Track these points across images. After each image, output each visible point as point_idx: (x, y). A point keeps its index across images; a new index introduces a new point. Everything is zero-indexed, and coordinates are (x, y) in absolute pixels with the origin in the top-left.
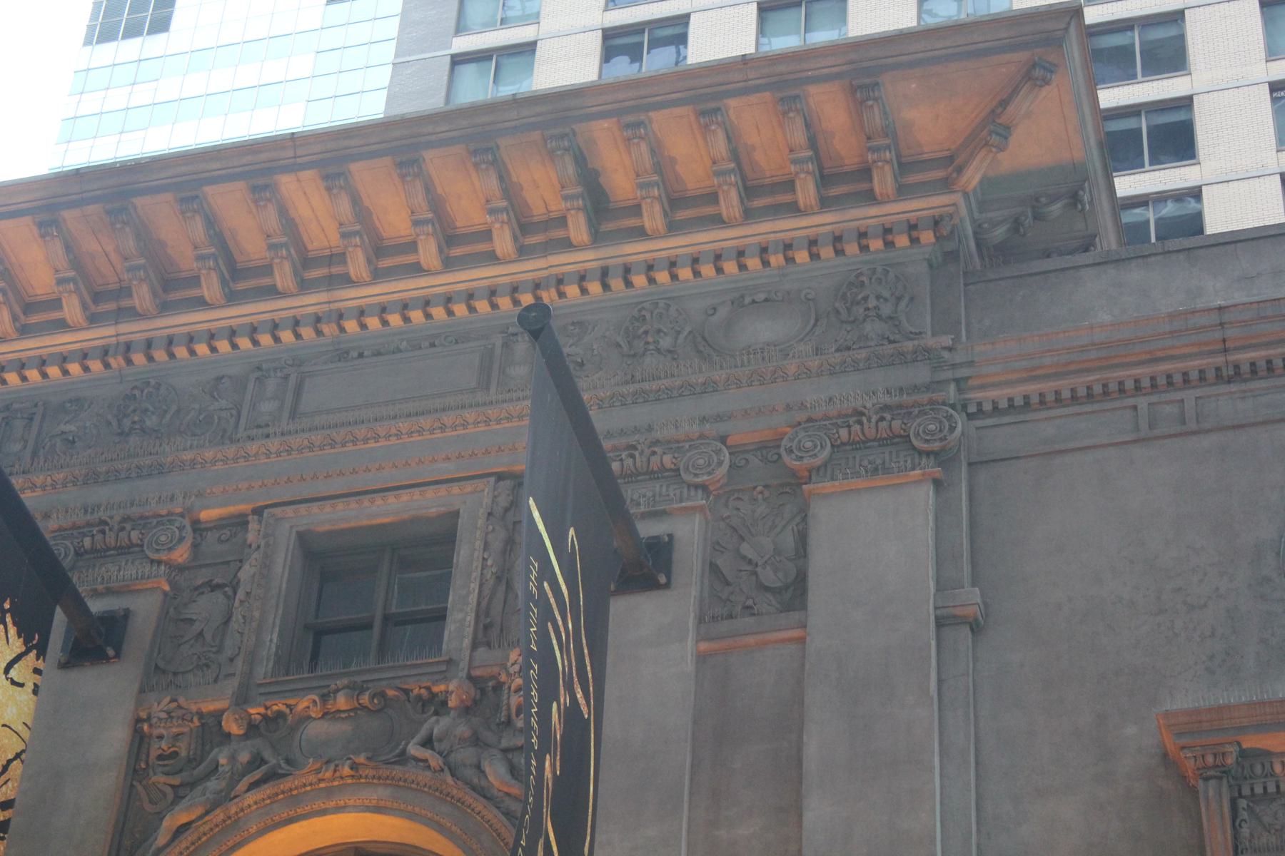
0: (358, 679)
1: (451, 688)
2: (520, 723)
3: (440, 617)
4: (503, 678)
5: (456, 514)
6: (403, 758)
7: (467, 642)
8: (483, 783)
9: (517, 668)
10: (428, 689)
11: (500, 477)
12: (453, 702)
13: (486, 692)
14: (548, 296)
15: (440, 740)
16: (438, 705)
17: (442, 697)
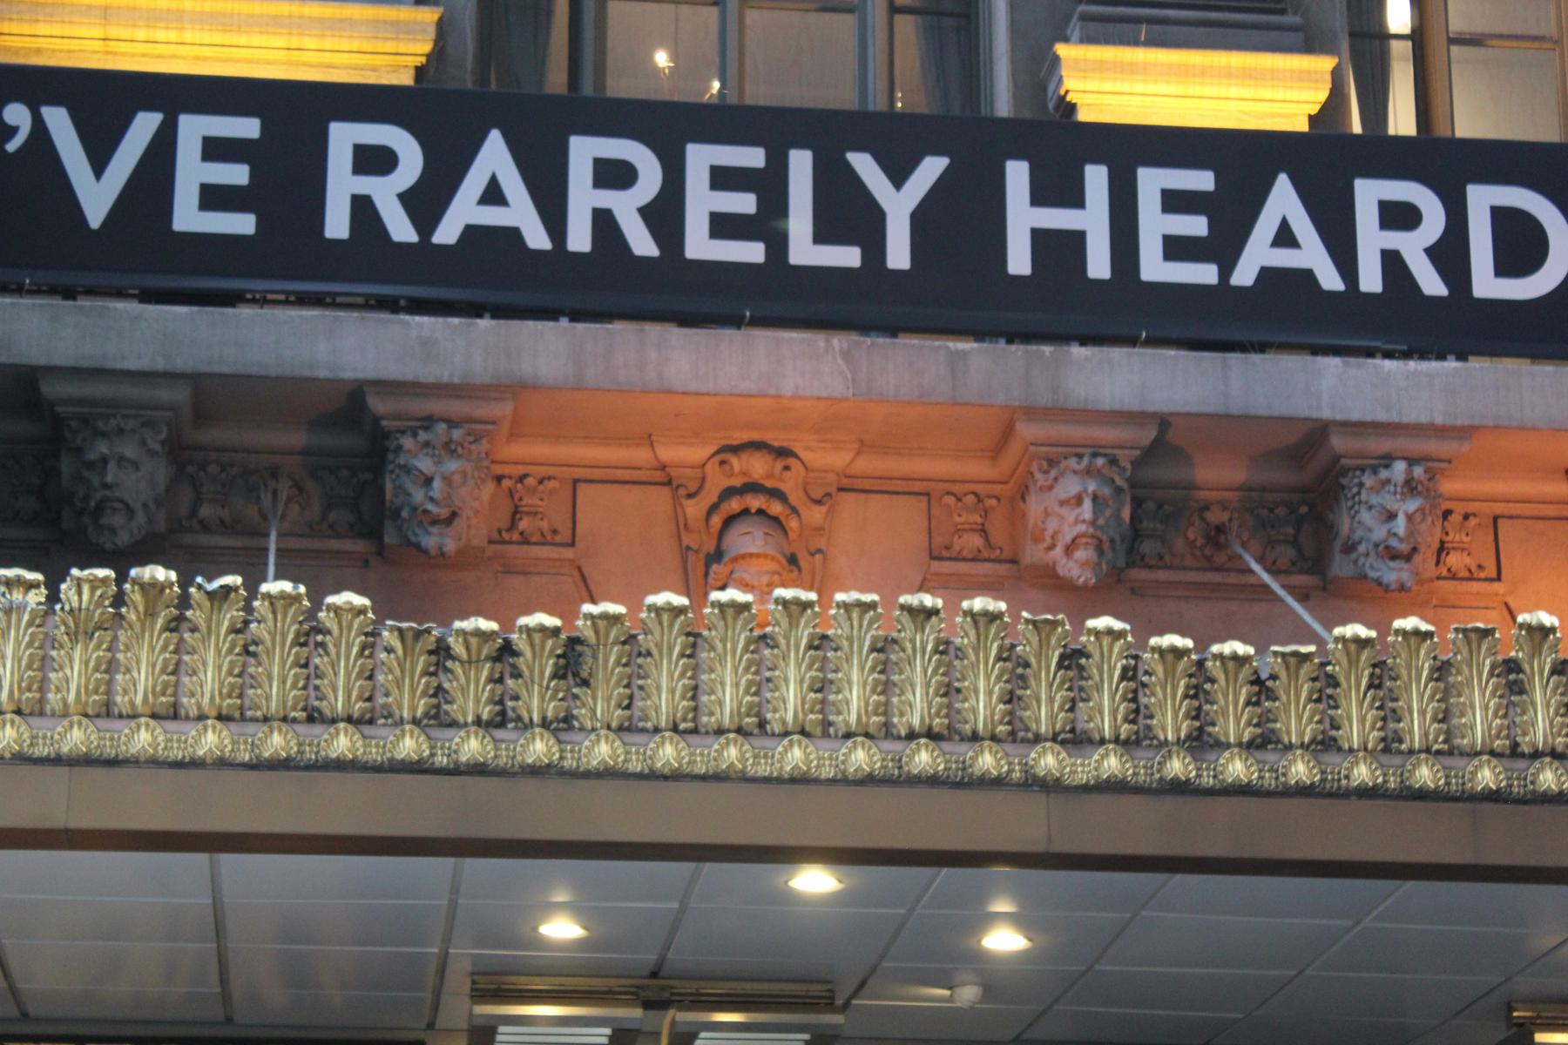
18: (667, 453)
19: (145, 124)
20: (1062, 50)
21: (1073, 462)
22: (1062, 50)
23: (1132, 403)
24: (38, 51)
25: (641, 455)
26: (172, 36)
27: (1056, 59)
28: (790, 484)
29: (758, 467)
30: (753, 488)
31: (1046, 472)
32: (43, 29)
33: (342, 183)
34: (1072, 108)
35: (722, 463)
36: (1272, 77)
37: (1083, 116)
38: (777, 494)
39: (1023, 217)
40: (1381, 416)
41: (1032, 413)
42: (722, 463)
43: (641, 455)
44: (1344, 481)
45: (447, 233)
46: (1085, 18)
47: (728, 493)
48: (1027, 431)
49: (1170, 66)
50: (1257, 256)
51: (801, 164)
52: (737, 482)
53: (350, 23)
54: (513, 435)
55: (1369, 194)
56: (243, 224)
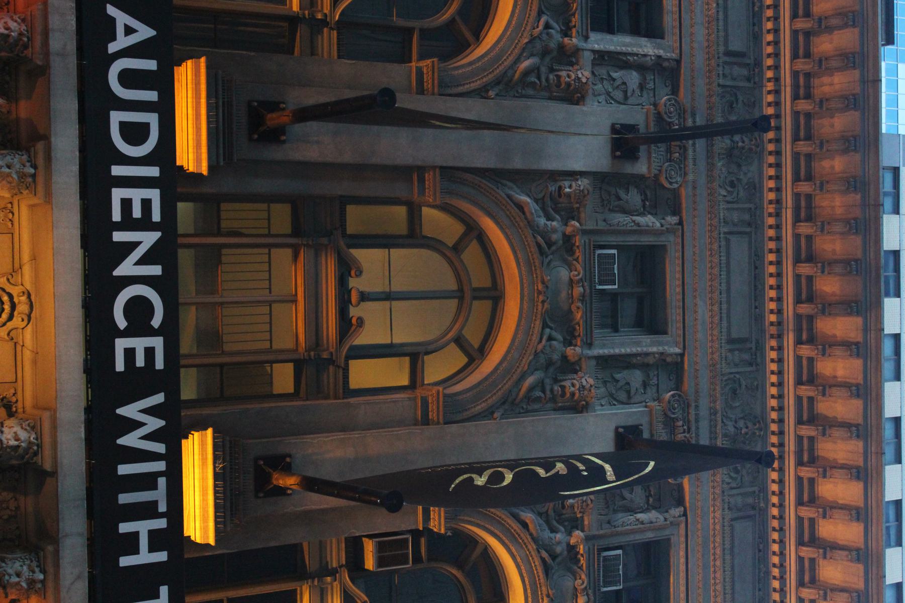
0: (587, 298)
1: (574, 40)
2: (556, 388)
3: (610, 31)
4: (576, 67)
5: (663, 38)
6: (540, 13)
7: (596, 47)
8: (523, 59)
9: (584, 383)
10: (579, 335)
11: (678, 62)
12: (566, 40)
13: (568, 57)
14: (771, 135)
15: (548, 34)
16: (566, 33)
17: (569, 33)
18: (27, 269)
20: (210, 431)
21: (33, 436)
22: (210, 431)
25: (26, 257)
27: (206, 429)
28: (17, 322)
29: (23, 308)
30: (13, 307)
31: (29, 425)
35: (24, 293)
36: (205, 519)
37: (184, 441)
38: (11, 317)
42: (24, 293)
43: (26, 257)
44: (33, 554)
47: (11, 296)
48: (46, 415)
52: (16, 300)
54: (32, 207)
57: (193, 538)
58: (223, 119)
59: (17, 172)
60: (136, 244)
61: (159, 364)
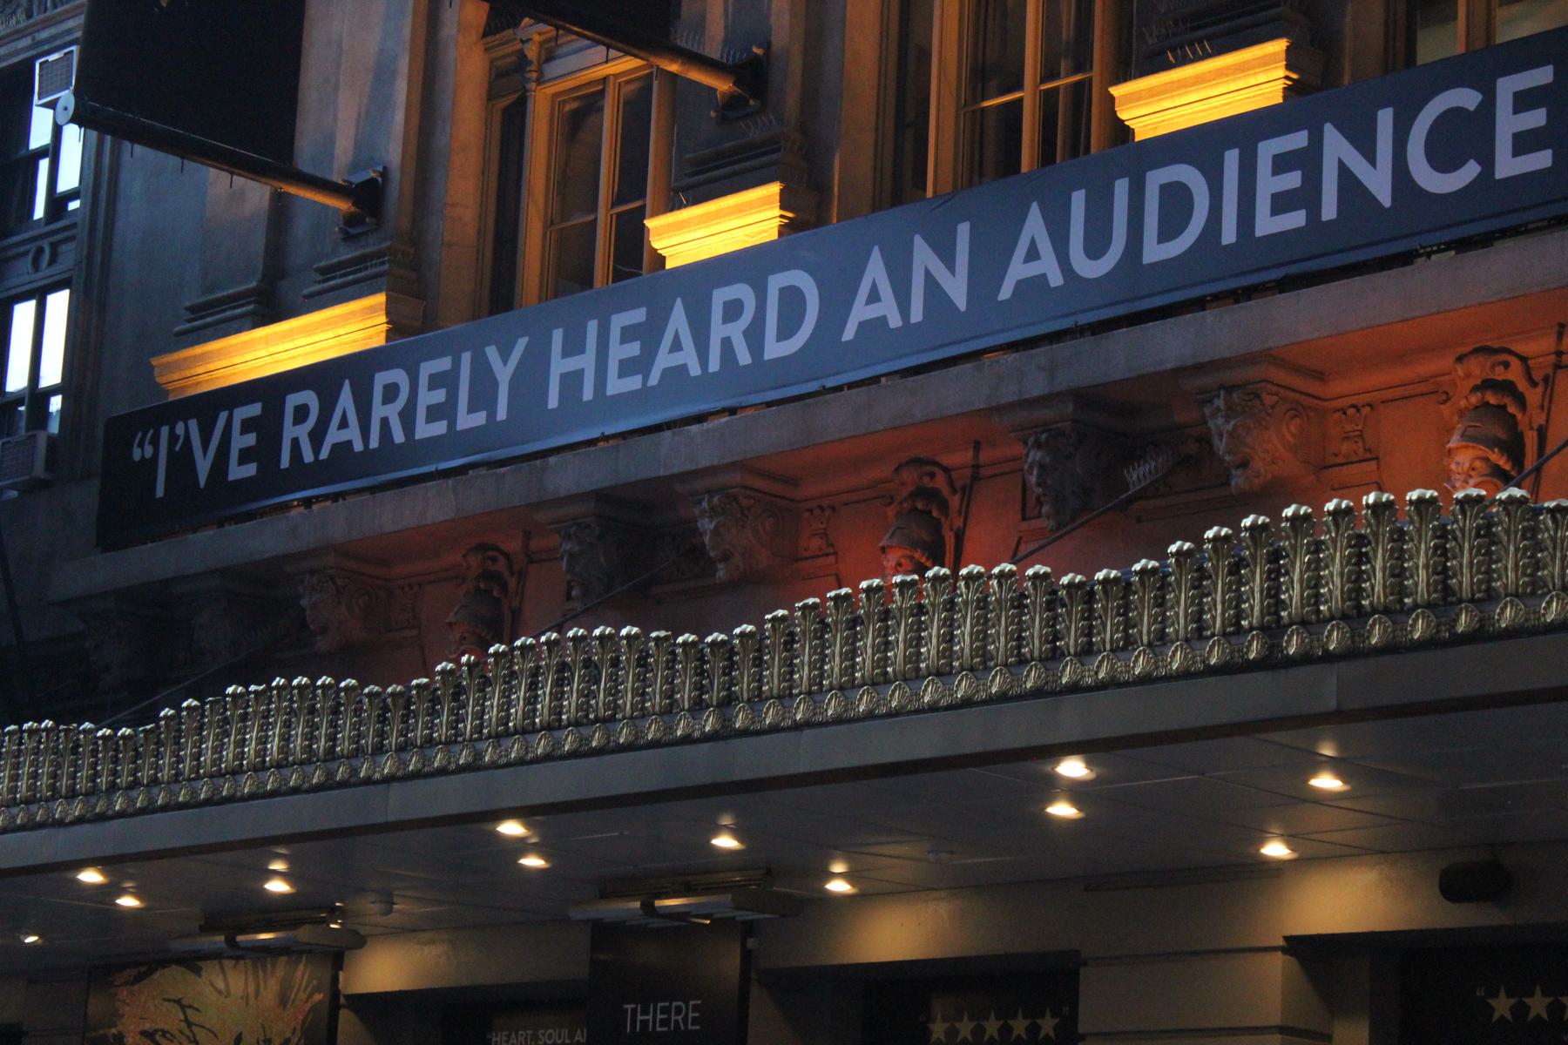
19: (224, 415)
23: (574, 490)
24: (251, 370)
26: (289, 345)
32: (248, 357)
33: (290, 431)
34: (663, 259)
39: (559, 366)
40: (689, 467)
41: (540, 505)
45: (324, 454)
46: (684, 190)
49: (700, 216)
50: (664, 360)
51: (466, 358)
53: (352, 314)
55: (720, 296)
56: (285, 462)
57: (385, 327)
58: (748, 159)
59: (1227, 422)
60: (1344, 170)
61: (1543, 76)
